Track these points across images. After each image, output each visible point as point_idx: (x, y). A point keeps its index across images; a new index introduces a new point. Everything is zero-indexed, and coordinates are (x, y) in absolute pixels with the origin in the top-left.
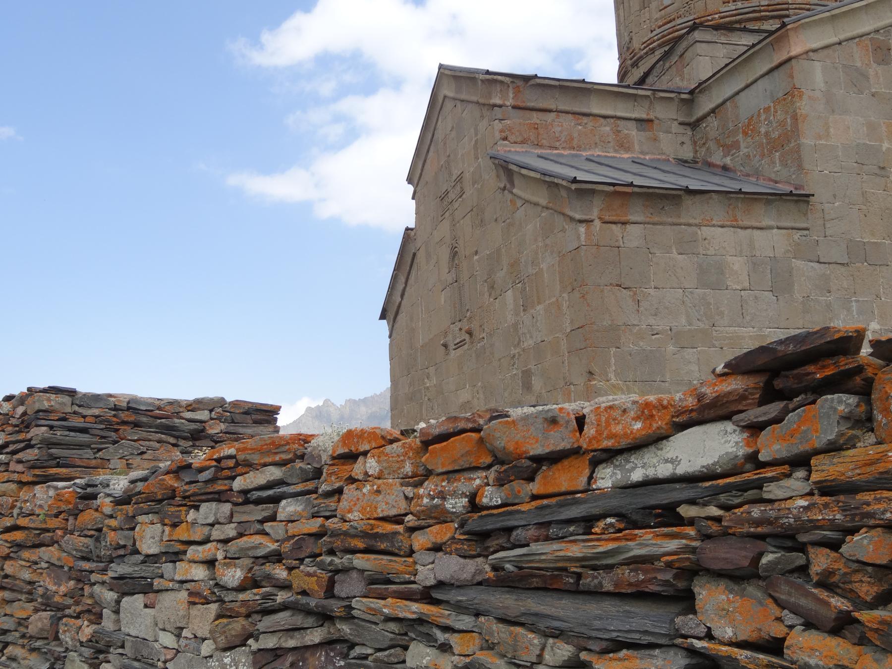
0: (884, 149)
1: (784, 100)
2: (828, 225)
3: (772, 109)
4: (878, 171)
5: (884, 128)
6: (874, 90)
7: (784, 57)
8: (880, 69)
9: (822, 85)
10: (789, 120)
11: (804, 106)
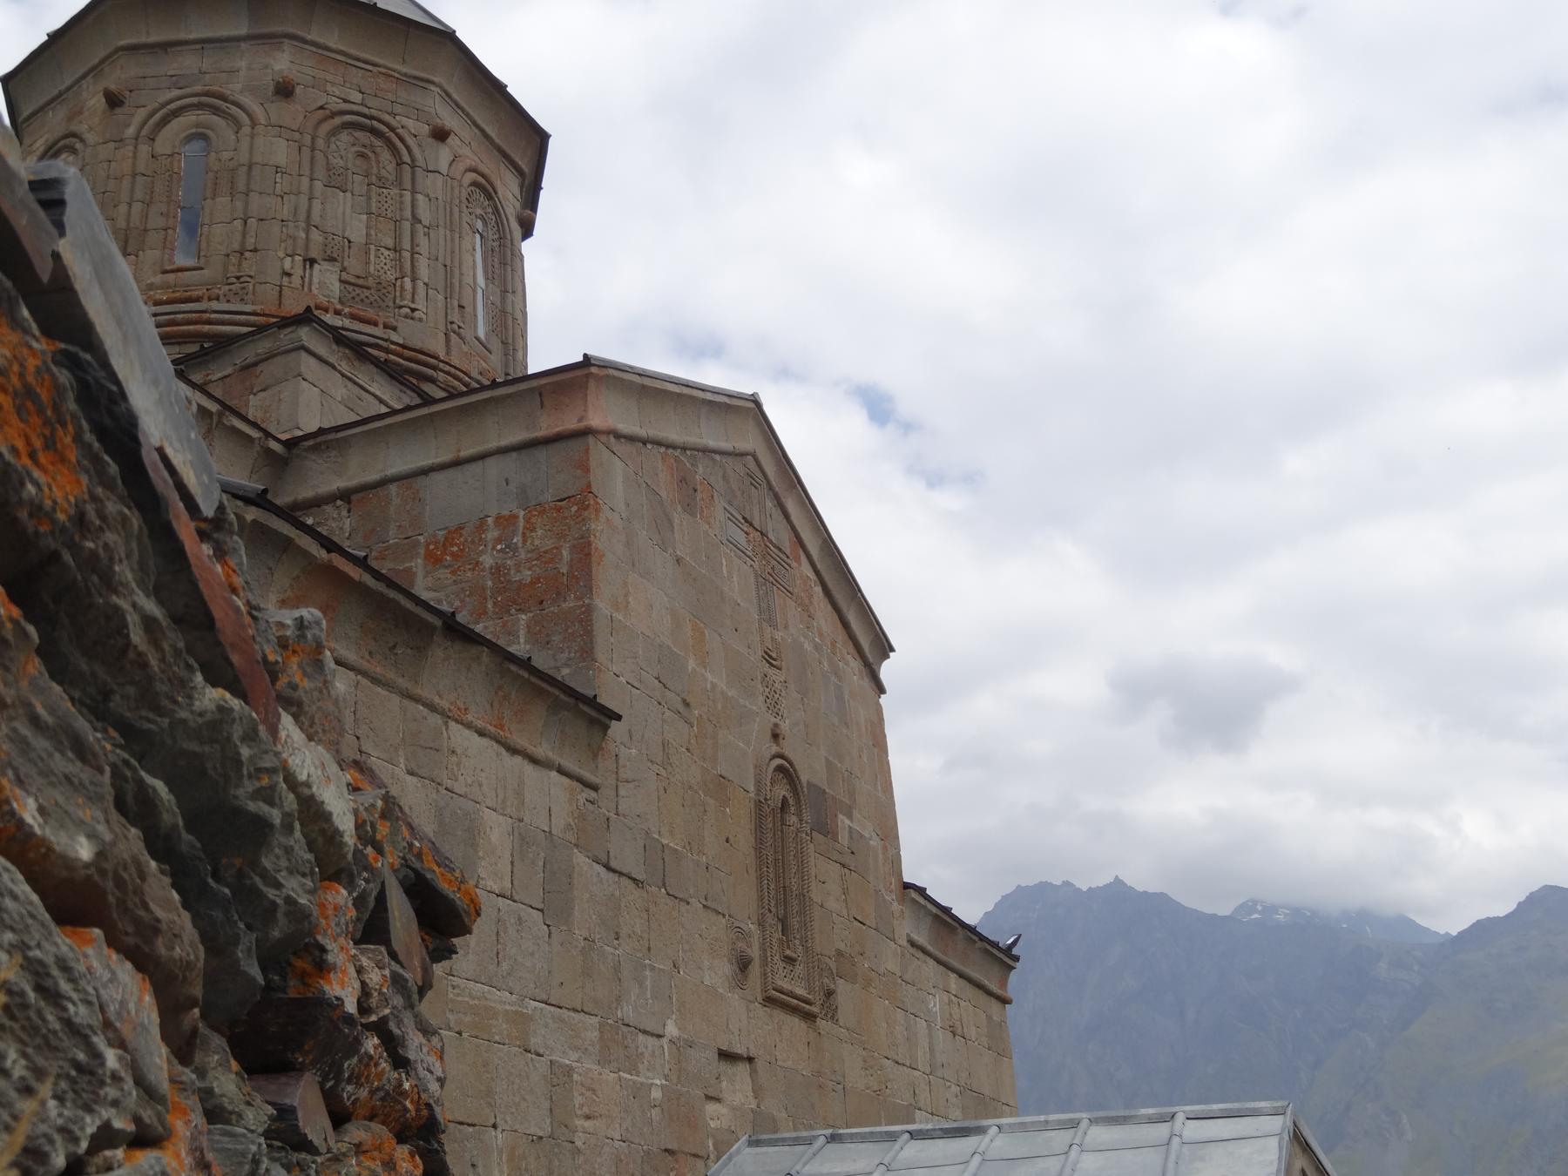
1: (559, 510)
2: (622, 792)
3: (521, 523)
7: (570, 423)
9: (622, 506)
10: (565, 553)
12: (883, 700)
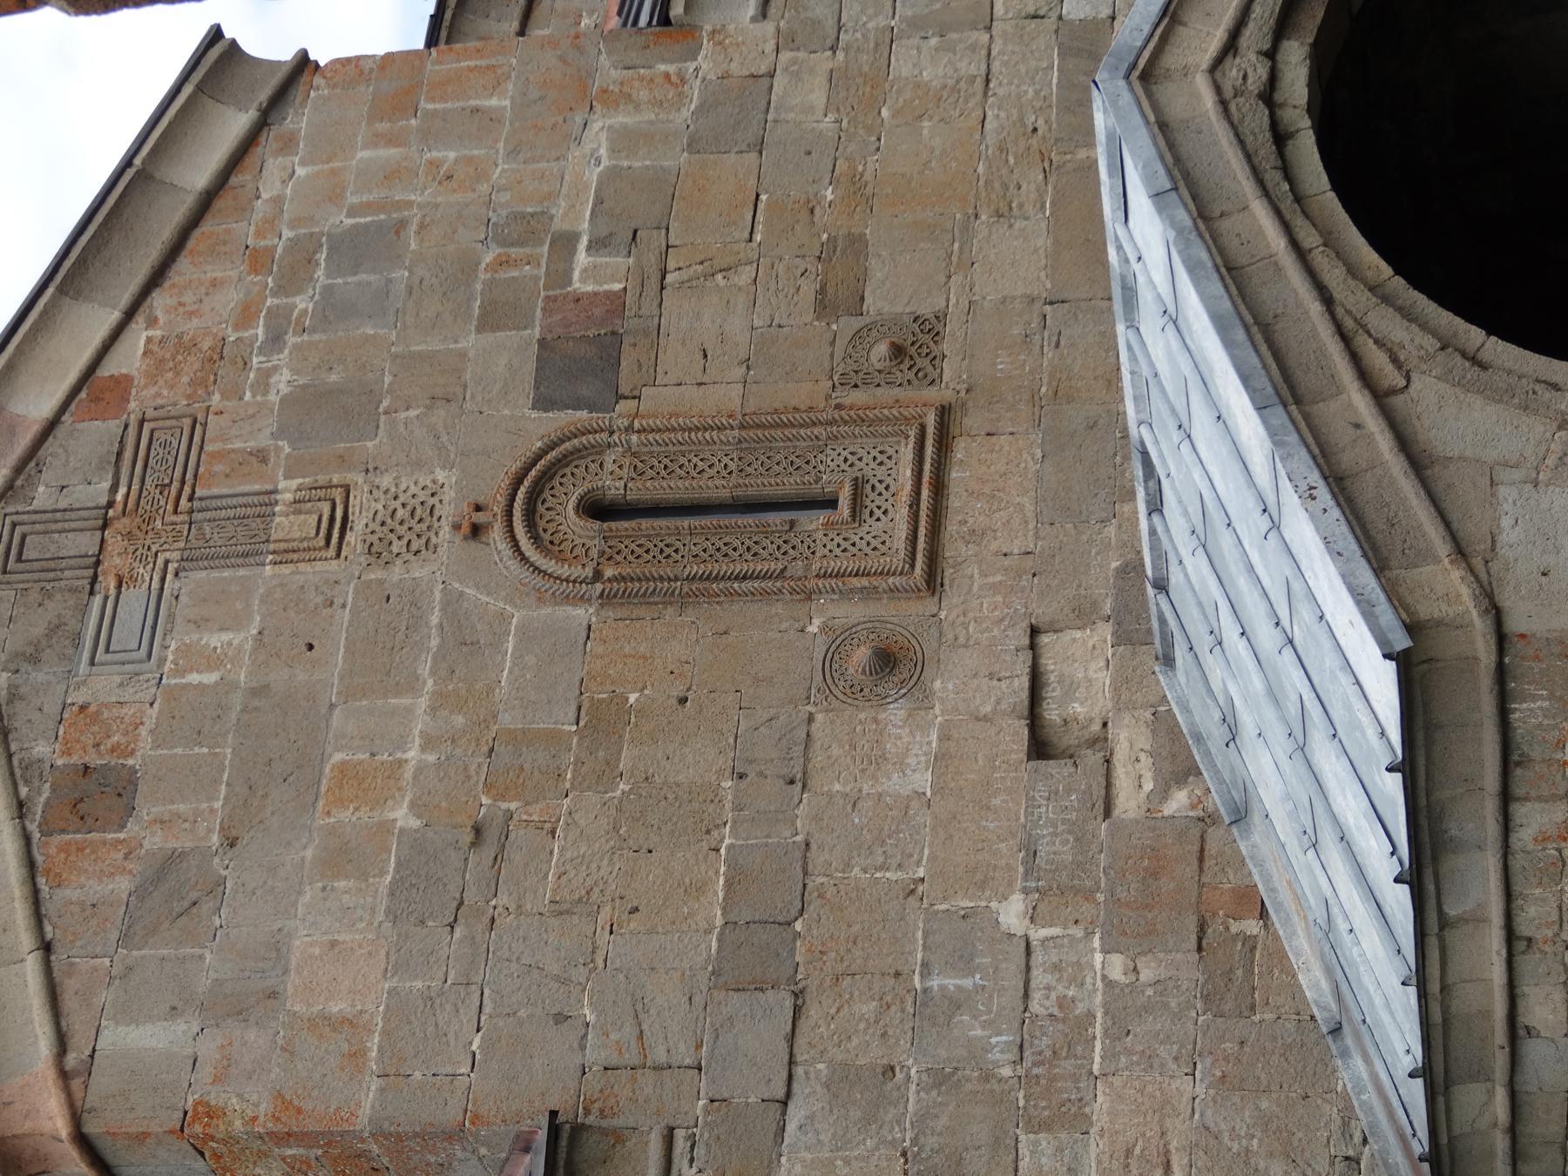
0: (414, 823)
2: (660, 1055)
4: (488, 852)
5: (345, 815)
6: (215, 839)
8: (147, 809)
9: (183, 1028)
10: (289, 1152)
11: (246, 1104)
12: (321, 56)
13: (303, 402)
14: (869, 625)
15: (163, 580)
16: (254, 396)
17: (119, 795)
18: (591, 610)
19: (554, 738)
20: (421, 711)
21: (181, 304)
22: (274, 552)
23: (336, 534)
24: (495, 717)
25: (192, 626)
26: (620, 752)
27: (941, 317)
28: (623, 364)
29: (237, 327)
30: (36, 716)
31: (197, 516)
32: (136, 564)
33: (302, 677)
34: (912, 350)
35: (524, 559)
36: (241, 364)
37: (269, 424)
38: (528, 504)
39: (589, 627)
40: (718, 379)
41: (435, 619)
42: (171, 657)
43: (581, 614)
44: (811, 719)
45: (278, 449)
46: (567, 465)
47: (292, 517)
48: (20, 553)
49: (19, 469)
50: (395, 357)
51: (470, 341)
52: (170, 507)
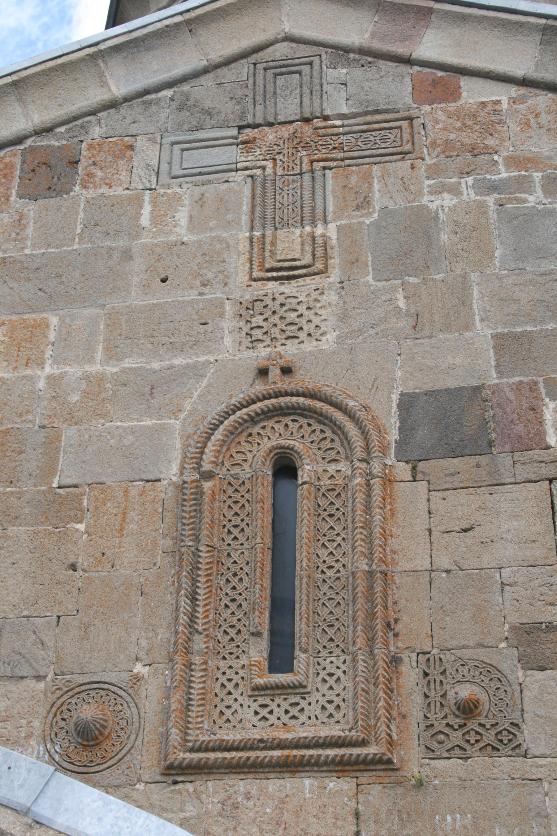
8: (31, 209)
13: (422, 224)
14: (136, 718)
15: (246, 169)
16: (429, 186)
17: (50, 188)
18: (174, 479)
19: (50, 470)
20: (87, 368)
21: (537, 116)
22: (263, 236)
23: (275, 274)
24: (76, 424)
25: (196, 198)
26: (27, 524)
27: (519, 751)
28: (456, 460)
29: (506, 159)
30: (128, 121)
31: (307, 178)
32: (264, 148)
33: (135, 280)
34: (473, 725)
35: (227, 414)
36: (468, 170)
37: (399, 203)
38: (288, 408)
39: (159, 480)
40: (435, 546)
41: (178, 361)
42: (169, 191)
43: (172, 471)
44: (39, 678)
45: (369, 214)
46: (334, 432)
47: (299, 240)
48: (282, 74)
49: (362, 51)
50: (465, 277)
51: (483, 332)
52: (316, 157)
